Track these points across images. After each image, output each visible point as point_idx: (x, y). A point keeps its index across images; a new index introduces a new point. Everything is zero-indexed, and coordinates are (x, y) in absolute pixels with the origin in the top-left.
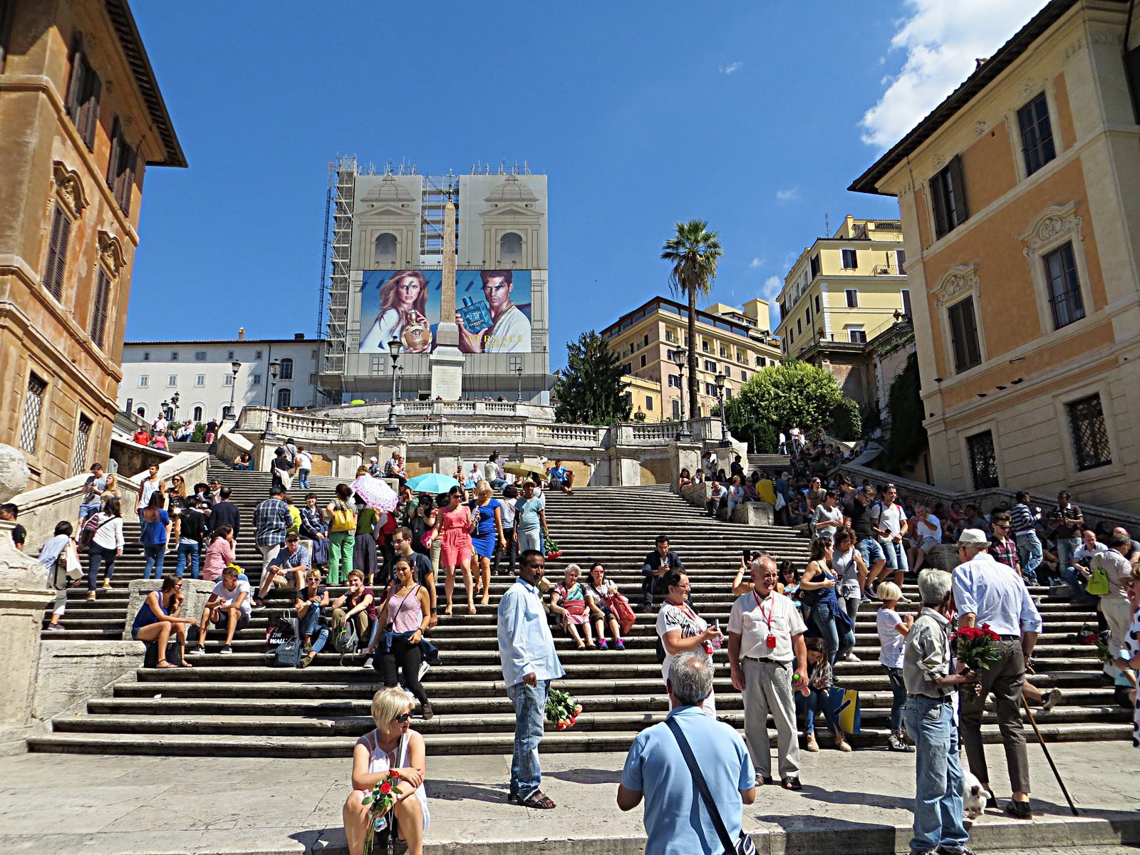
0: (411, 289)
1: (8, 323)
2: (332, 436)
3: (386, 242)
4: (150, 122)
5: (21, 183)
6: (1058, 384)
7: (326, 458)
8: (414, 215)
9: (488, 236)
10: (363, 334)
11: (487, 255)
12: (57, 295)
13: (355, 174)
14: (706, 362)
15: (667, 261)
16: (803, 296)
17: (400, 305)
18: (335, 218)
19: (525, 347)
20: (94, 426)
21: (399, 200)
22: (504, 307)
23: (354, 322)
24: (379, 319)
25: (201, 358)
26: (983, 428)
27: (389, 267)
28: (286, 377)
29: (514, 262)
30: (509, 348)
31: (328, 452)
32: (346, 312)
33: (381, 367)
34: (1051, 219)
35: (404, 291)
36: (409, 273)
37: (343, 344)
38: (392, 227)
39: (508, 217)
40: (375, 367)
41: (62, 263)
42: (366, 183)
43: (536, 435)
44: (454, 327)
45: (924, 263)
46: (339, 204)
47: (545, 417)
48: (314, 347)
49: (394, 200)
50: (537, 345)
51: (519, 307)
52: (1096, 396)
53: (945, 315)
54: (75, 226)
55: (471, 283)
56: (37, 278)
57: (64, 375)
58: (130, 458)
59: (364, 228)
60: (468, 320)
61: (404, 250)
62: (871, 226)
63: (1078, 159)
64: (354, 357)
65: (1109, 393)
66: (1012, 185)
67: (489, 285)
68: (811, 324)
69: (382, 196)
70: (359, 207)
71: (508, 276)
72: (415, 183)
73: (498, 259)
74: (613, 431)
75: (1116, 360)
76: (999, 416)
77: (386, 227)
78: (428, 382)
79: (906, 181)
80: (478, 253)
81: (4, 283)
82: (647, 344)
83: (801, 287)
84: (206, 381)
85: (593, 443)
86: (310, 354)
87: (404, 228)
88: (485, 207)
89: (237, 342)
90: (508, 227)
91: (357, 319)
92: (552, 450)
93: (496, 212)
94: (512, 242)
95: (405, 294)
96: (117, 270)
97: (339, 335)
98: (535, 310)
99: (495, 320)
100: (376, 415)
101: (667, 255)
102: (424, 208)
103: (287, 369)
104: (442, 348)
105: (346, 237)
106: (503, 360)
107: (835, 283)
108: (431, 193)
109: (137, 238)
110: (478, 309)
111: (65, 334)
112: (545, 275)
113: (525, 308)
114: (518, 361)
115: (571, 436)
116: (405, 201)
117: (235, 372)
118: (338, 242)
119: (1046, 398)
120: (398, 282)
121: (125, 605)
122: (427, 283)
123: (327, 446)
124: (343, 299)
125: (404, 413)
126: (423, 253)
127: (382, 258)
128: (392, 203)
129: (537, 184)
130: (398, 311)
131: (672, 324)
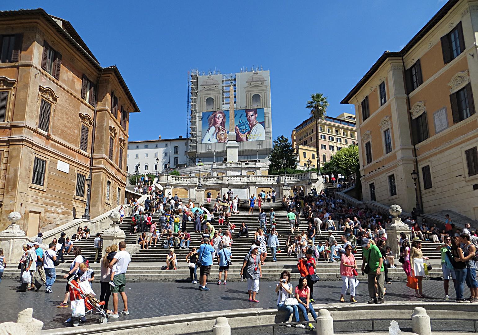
0: (219, 118)
1: (103, 171)
2: (188, 182)
3: (210, 101)
4: (130, 103)
5: (103, 135)
7: (186, 190)
8: (219, 90)
9: (247, 96)
10: (203, 137)
11: (247, 104)
12: (112, 160)
13: (198, 76)
14: (337, 138)
15: (308, 109)
17: (216, 125)
18: (191, 93)
19: (263, 138)
20: (121, 190)
21: (214, 84)
22: (254, 123)
23: (199, 132)
24: (208, 130)
25: (146, 147)
27: (211, 110)
28: (177, 153)
29: (258, 106)
30: (257, 138)
31: (187, 188)
32: (196, 128)
33: (210, 148)
34: (385, 121)
35: (217, 119)
36: (219, 112)
37: (196, 140)
38: (212, 95)
39: (255, 88)
40: (208, 149)
41: (112, 151)
42: (202, 79)
43: (254, 180)
44: (234, 134)
45: (360, 129)
46: (192, 88)
48: (185, 141)
49: (212, 85)
51: (260, 123)
53: (365, 145)
54: (114, 140)
55: (242, 115)
56: (107, 157)
57: (114, 179)
58: (129, 196)
59: (202, 96)
60: (241, 129)
61: (216, 103)
63: (390, 104)
64: (200, 145)
65: (396, 174)
66: (378, 108)
67: (249, 115)
69: (208, 84)
70: (200, 88)
71: (255, 111)
72: (219, 78)
73: (252, 105)
74: (280, 177)
76: (376, 178)
78: (225, 154)
79: (356, 102)
80: (244, 102)
81: (101, 161)
82: (312, 133)
84: (149, 155)
85: (273, 181)
86: (184, 144)
87: (216, 95)
89: (159, 141)
90: (255, 92)
91: (200, 130)
92: (259, 184)
93: (251, 86)
94: (257, 98)
96: (124, 147)
97: (194, 137)
98: (266, 124)
99: (251, 128)
100: (207, 169)
101: (308, 107)
102: (223, 87)
103: (176, 150)
105: (195, 100)
106: (254, 144)
108: (226, 81)
109: (128, 136)
110: (245, 124)
111: (114, 168)
112: (270, 110)
113: (262, 123)
116: (216, 85)
117: (157, 162)
118: (192, 102)
119: (384, 174)
120: (215, 116)
121: (136, 238)
122: (225, 116)
123: (186, 185)
124: (195, 124)
126: (223, 104)
128: (212, 86)
129: (265, 74)
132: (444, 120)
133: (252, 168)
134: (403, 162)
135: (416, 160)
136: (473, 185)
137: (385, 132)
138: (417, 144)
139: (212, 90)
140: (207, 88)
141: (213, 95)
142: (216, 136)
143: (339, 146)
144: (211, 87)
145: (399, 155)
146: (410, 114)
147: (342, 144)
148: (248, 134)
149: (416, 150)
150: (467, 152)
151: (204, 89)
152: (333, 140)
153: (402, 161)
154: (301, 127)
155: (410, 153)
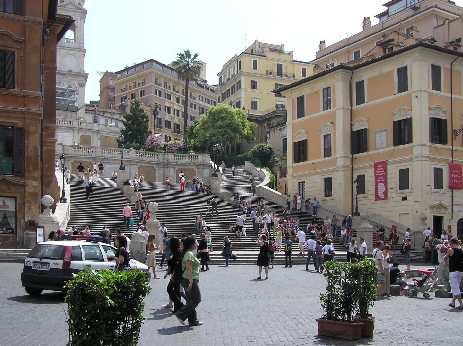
6: (323, 172)
16: (233, 79)
26: (303, 180)
34: (327, 126)
43: (135, 156)
45: (292, 124)
47: (107, 131)
52: (331, 178)
62: (267, 49)
65: (334, 178)
66: (319, 111)
68: (234, 94)
75: (336, 170)
83: (232, 73)
107: (247, 74)
115: (149, 157)
119: (320, 176)
132: (385, 141)
134: (344, 169)
135: (352, 168)
136: (402, 197)
137: (325, 136)
138: (355, 154)
143: (176, 107)
145: (340, 162)
146: (352, 125)
147: (180, 106)
149: (354, 159)
150: (401, 171)
152: (170, 99)
153: (343, 168)
155: (349, 162)
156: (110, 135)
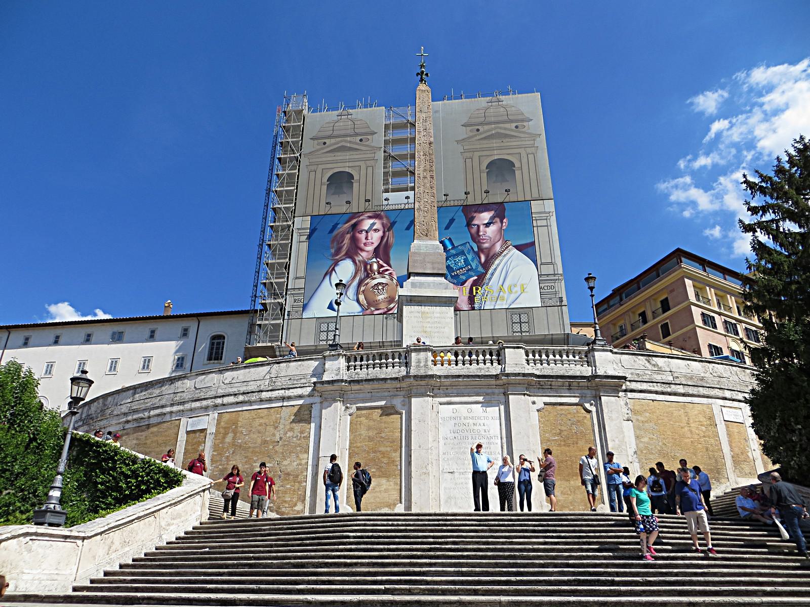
0: (371, 234)
8: (376, 149)
10: (308, 295)
13: (305, 112)
17: (357, 254)
18: (280, 159)
19: (532, 298)
21: (357, 135)
22: (498, 248)
23: (297, 278)
24: (329, 273)
25: (118, 338)
27: (344, 209)
30: (509, 302)
32: (287, 267)
35: (362, 236)
36: (369, 214)
37: (282, 308)
38: (347, 164)
40: (323, 336)
47: (658, 378)
49: (351, 136)
50: (549, 296)
55: (452, 221)
59: (313, 168)
61: (362, 188)
64: (295, 323)
67: (476, 222)
69: (335, 133)
70: (308, 146)
71: (500, 210)
73: (485, 188)
77: (340, 165)
87: (362, 164)
88: (463, 133)
93: (478, 137)
95: (364, 241)
97: (276, 296)
98: (542, 250)
99: (486, 266)
102: (386, 142)
103: (218, 349)
104: (416, 278)
110: (462, 253)
112: (550, 206)
113: (527, 249)
114: (524, 318)
118: (282, 185)
120: (355, 226)
122: (393, 224)
125: (345, 375)
126: (387, 191)
127: (334, 200)
128: (349, 139)
130: (354, 262)
131: (700, 282)
133: (569, 382)
139: (350, 149)
140: (335, 144)
141: (351, 164)
142: (357, 294)
144: (346, 141)
148: (475, 283)
151: (322, 149)
154: (618, 298)
156: (675, 394)
